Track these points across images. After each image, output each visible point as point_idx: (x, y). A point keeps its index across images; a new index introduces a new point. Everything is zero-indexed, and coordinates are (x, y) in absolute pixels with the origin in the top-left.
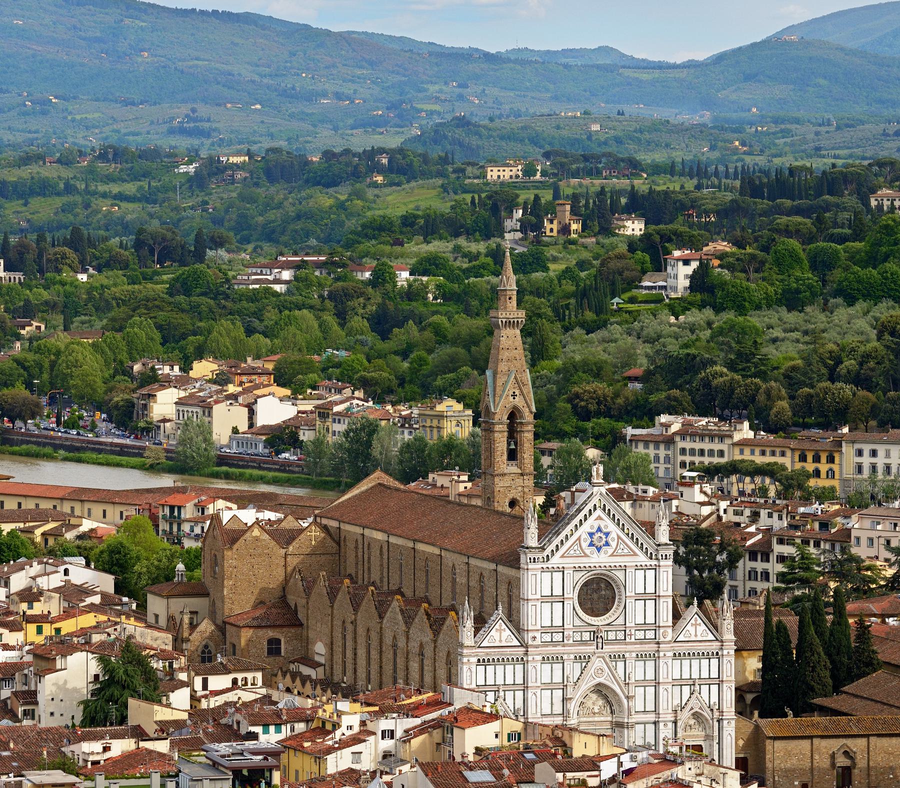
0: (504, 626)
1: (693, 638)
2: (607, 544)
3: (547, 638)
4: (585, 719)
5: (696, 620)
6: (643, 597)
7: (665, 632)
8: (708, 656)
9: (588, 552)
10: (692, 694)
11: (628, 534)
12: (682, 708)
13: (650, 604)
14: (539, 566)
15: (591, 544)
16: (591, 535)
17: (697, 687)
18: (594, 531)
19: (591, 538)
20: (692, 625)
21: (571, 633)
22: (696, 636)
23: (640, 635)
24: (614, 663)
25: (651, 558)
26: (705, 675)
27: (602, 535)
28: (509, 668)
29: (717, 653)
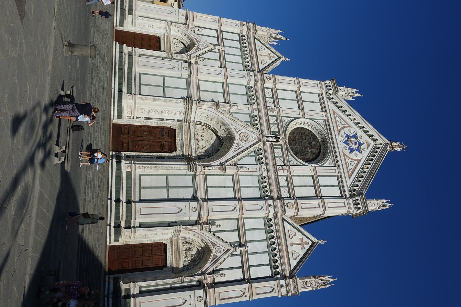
0: (273, 59)
1: (289, 243)
2: (352, 150)
3: (268, 93)
4: (192, 130)
6: (316, 185)
8: (273, 264)
9: (342, 132)
12: (214, 233)
13: (311, 192)
15: (348, 137)
16: (355, 136)
17: (238, 252)
18: (359, 140)
21: (275, 114)
22: (292, 245)
24: (253, 154)
26: (253, 260)
27: (357, 145)
28: (239, 59)
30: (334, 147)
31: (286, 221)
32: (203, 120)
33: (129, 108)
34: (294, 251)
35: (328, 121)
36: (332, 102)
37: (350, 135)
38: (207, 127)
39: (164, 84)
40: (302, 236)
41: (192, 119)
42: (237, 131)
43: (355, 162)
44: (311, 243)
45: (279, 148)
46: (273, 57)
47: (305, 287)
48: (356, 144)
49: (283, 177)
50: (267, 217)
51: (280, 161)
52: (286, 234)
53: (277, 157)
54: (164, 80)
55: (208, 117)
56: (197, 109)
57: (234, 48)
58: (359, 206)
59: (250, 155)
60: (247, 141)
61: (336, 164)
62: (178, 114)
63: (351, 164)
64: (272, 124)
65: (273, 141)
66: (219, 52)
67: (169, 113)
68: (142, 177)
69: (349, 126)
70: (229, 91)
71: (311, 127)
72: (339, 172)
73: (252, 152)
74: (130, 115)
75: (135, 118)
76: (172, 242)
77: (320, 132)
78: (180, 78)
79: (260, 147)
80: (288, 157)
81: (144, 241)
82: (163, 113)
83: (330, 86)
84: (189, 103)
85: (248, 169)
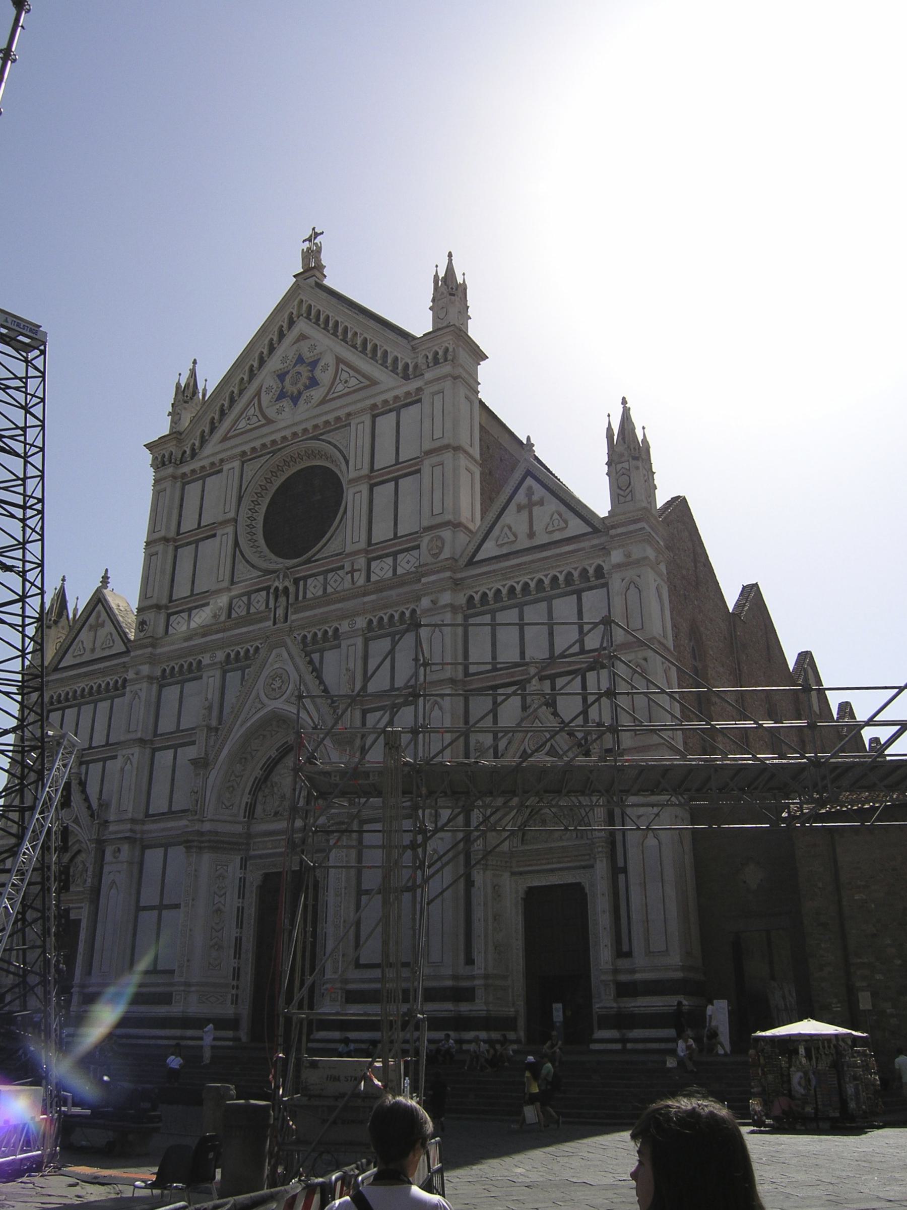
1: (527, 544)
2: (314, 382)
4: (264, 827)
5: (530, 492)
7: (431, 540)
9: (271, 412)
10: (524, 708)
11: (354, 346)
14: (170, 470)
15: (282, 396)
16: (281, 377)
19: (282, 381)
20: (520, 508)
22: (531, 535)
23: (382, 570)
25: (406, 377)
29: (599, 570)
30: (305, 430)
31: (474, 555)
32: (241, 798)
33: (207, 999)
34: (546, 528)
35: (244, 453)
36: (201, 446)
37: (279, 390)
38: (261, 788)
39: (152, 908)
40: (512, 507)
41: (239, 829)
42: (260, 706)
43: (342, 370)
44: (529, 481)
45: (305, 585)
46: (98, 616)
47: (631, 491)
48: (299, 373)
49: (372, 570)
50: (465, 609)
51: (336, 581)
52: (505, 552)
53: (325, 589)
54: (145, 908)
55: (232, 786)
56: (209, 817)
57: (77, 725)
58: (441, 353)
59: (317, 665)
60: (283, 676)
61: (342, 423)
62: (225, 867)
63: (346, 382)
64: (248, 609)
65: (285, 603)
66: (87, 763)
67: (223, 892)
68: (361, 962)
69: (258, 394)
70: (172, 733)
71: (262, 497)
72: (363, 410)
73: (311, 662)
74: (229, 997)
75: (235, 983)
76: (521, 873)
77: (272, 472)
78: (141, 864)
79: (299, 638)
80: (326, 558)
81: (517, 949)
82: (222, 907)
83: (164, 456)
84: (193, 841)
85: (348, 670)
